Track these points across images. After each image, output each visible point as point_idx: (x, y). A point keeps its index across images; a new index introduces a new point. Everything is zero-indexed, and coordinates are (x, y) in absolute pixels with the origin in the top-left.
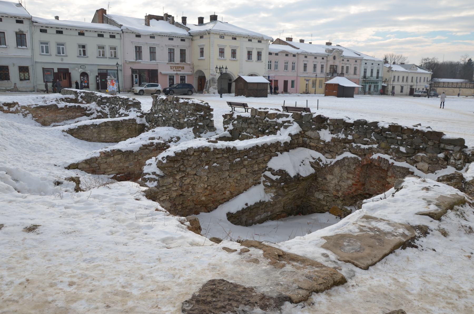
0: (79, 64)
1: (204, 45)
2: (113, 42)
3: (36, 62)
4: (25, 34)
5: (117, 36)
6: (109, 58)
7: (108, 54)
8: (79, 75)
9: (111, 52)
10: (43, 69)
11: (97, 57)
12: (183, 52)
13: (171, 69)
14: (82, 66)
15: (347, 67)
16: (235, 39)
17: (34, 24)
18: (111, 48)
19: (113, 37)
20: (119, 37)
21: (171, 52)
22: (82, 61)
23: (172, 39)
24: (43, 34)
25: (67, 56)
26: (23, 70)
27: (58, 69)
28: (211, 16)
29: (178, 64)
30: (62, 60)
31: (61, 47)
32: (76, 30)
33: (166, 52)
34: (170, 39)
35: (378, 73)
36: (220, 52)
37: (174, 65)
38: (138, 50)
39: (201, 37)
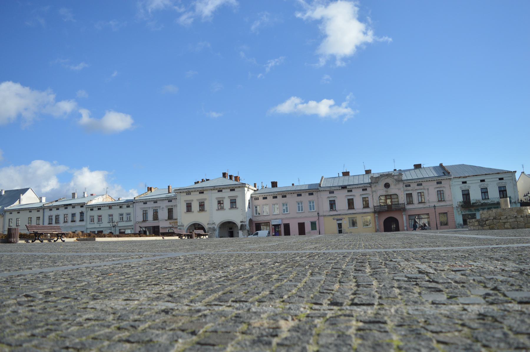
2: (129, 210)
5: (131, 206)
6: (126, 221)
7: (125, 219)
9: (128, 217)
16: (203, 193)
19: (128, 207)
23: (171, 201)
25: (102, 223)
30: (100, 226)
31: (100, 217)
32: (107, 206)
33: (166, 212)
34: (169, 201)
36: (187, 206)
38: (145, 214)
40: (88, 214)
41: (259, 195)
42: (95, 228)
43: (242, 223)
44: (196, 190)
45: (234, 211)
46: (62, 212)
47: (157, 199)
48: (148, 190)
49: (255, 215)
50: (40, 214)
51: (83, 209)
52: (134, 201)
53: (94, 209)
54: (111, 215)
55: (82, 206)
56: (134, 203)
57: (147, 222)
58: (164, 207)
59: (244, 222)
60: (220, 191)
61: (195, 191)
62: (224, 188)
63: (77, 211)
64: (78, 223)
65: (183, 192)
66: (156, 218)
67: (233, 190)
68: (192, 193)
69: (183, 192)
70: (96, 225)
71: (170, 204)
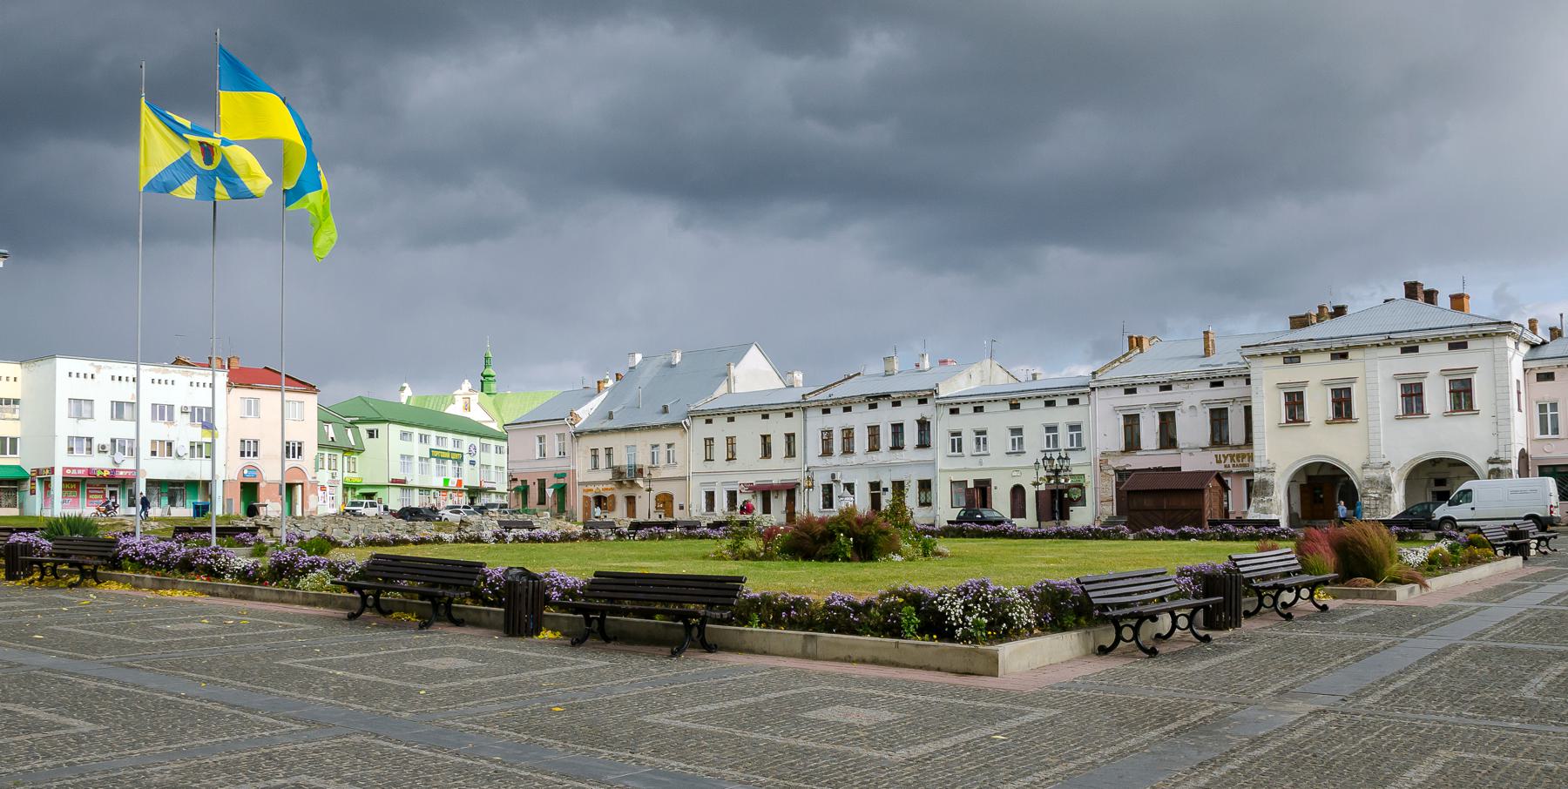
4: (929, 422)
5: (1083, 400)
9: (1072, 436)
13: (1219, 462)
16: (1344, 356)
23: (1221, 384)
27: (976, 482)
29: (1238, 447)
34: (1214, 385)
37: (1226, 453)
38: (1132, 422)
41: (1558, 362)
42: (965, 470)
43: (1495, 466)
44: (1322, 347)
45: (1462, 422)
46: (860, 420)
47: (1174, 377)
48: (1131, 347)
50: (793, 425)
51: (926, 411)
52: (1092, 385)
53: (963, 409)
55: (923, 401)
56: (1093, 389)
57: (1138, 453)
58: (1197, 404)
59: (1503, 462)
60: (1410, 349)
61: (1316, 351)
62: (1426, 341)
63: (909, 414)
64: (910, 453)
65: (1273, 354)
66: (1168, 440)
67: (1458, 345)
68: (1304, 359)
69: (1273, 354)
71: (1218, 393)
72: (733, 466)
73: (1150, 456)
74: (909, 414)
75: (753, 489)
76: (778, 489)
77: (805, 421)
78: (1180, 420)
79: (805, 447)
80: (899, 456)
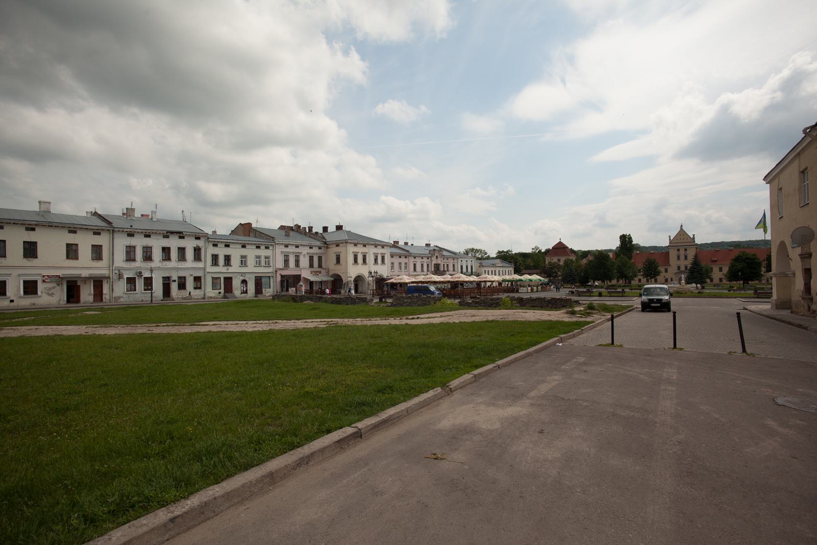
0: (241, 273)
1: (340, 252)
3: (208, 272)
5: (271, 248)
6: (264, 266)
7: (263, 263)
8: (240, 282)
9: (266, 261)
10: (213, 278)
11: (255, 266)
12: (320, 258)
14: (242, 274)
15: (447, 265)
16: (365, 246)
17: (210, 240)
18: (266, 258)
20: (272, 248)
21: (311, 258)
22: (244, 270)
23: (312, 248)
24: (215, 248)
26: (197, 279)
28: (337, 226)
30: (228, 269)
33: (307, 259)
34: (310, 248)
35: (472, 269)
39: (338, 245)
40: (209, 251)
49: (413, 274)
50: (103, 240)
51: (200, 243)
54: (258, 257)
63: (189, 244)
70: (221, 269)
72: (34, 262)
73: (292, 271)
74: (189, 244)
75: (59, 280)
76: (86, 280)
77: (113, 239)
78: (301, 258)
79: (113, 255)
80: (182, 265)
